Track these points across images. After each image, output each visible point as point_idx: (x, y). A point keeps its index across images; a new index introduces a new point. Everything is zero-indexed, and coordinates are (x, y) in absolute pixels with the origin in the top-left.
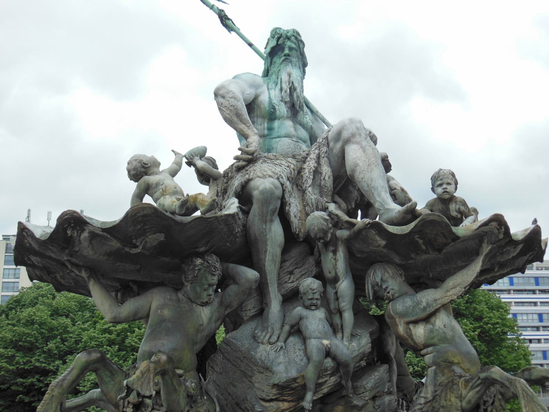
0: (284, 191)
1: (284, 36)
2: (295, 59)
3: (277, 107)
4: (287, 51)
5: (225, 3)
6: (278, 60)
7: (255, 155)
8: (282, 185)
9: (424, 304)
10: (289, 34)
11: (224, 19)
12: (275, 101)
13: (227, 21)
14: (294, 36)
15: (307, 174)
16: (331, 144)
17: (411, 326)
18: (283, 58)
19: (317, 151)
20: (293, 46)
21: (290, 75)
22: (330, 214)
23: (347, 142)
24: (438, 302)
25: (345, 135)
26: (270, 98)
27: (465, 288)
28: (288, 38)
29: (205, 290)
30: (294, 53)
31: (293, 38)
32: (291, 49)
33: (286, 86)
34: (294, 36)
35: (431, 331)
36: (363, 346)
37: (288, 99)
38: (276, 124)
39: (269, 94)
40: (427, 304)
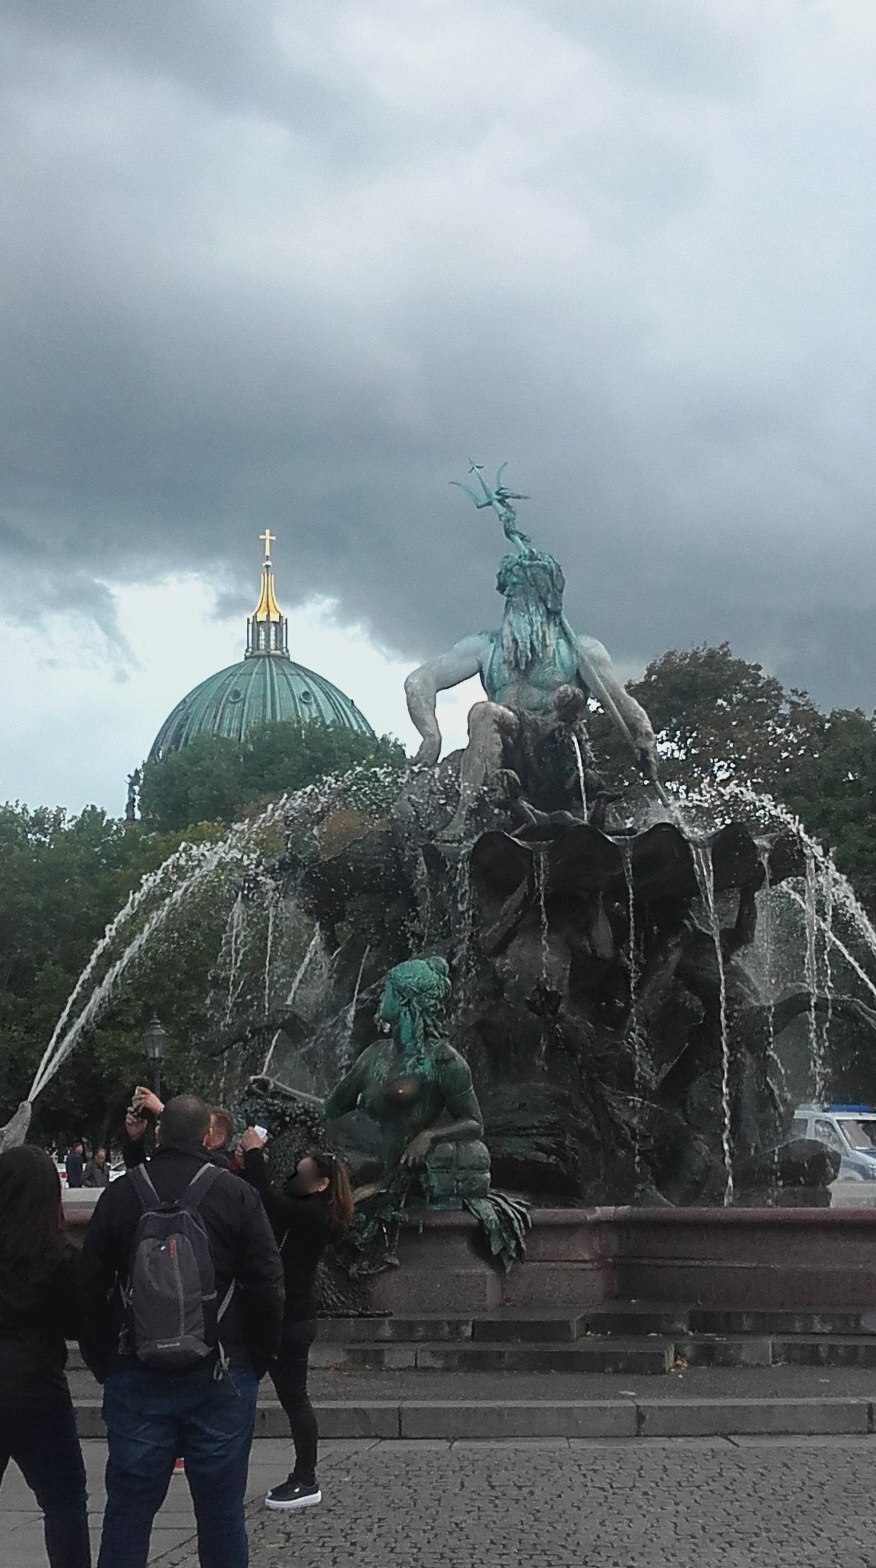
5: (526, 498)
20: (515, 580)
34: (517, 564)
37: (512, 659)
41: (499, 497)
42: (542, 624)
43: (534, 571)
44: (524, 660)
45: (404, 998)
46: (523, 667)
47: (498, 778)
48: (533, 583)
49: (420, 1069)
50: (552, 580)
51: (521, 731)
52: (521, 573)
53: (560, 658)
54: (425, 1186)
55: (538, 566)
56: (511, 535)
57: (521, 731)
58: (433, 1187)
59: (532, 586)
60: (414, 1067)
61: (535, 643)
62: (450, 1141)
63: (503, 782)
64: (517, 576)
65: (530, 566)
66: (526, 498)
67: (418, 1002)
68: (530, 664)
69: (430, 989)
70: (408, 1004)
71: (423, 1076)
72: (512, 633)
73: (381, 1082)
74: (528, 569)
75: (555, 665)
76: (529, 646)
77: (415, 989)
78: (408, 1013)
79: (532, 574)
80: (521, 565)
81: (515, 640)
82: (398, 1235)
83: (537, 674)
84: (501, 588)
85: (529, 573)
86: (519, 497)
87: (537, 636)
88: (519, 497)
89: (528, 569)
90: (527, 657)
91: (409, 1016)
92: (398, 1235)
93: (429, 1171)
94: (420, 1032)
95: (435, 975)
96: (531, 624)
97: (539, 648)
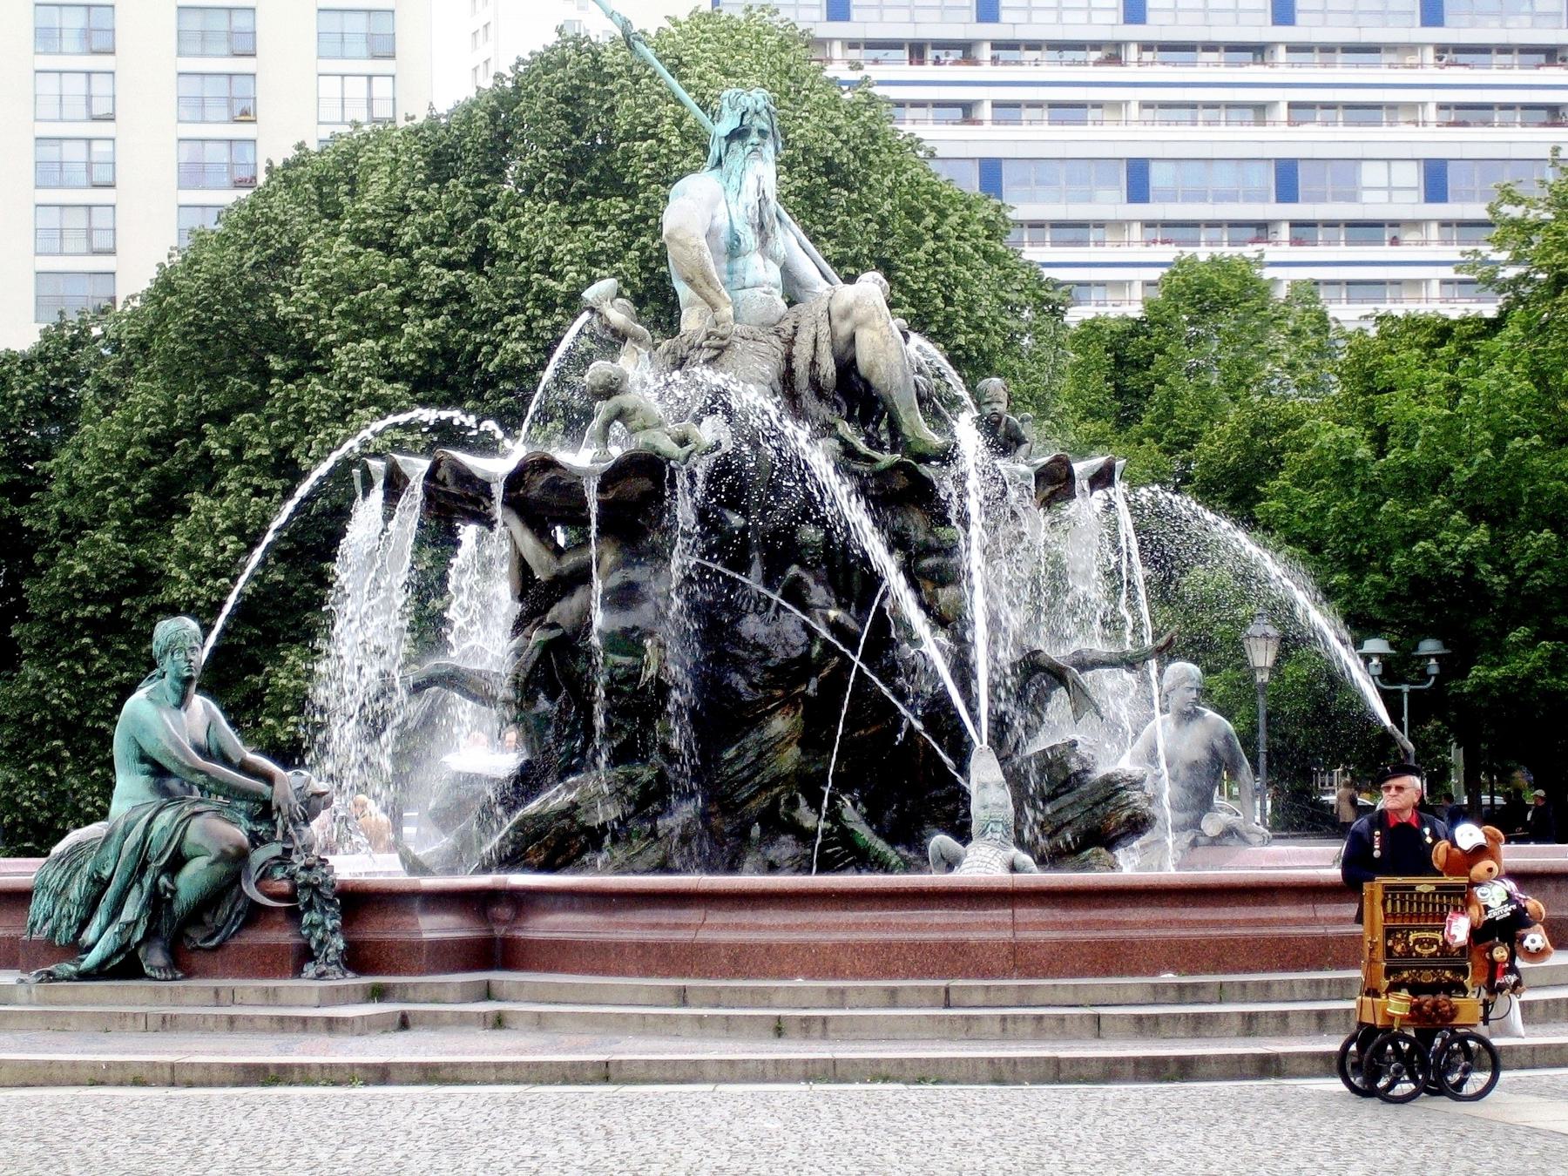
1: (751, 111)
4: (754, 138)
6: (735, 145)
10: (759, 107)
12: (738, 226)
15: (801, 365)
16: (835, 321)
18: (750, 148)
19: (813, 331)
20: (766, 127)
22: (843, 442)
23: (860, 324)
25: (859, 313)
28: (757, 113)
32: (762, 133)
38: (740, 264)
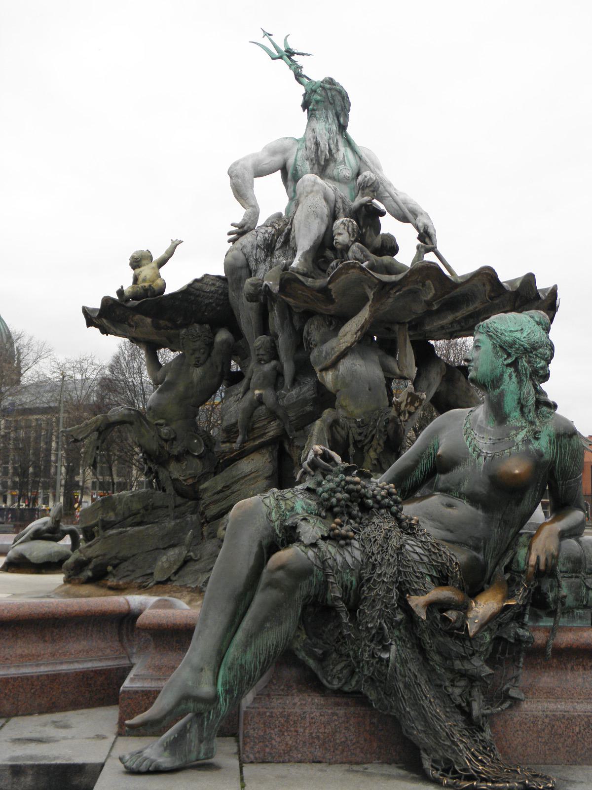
0: (247, 260)
2: (320, 112)
3: (299, 168)
5: (309, 55)
7: (246, 228)
8: (245, 255)
9: (324, 353)
11: (299, 76)
12: (299, 163)
13: (300, 78)
14: (321, 86)
17: (324, 373)
20: (319, 98)
21: (314, 131)
24: (336, 349)
26: (296, 160)
27: (356, 333)
29: (192, 354)
30: (321, 105)
31: (319, 91)
32: (317, 102)
33: (310, 144)
35: (337, 377)
36: (303, 394)
39: (297, 154)
40: (326, 352)
41: (287, 54)
42: (336, 133)
43: (334, 93)
44: (323, 157)
45: (509, 355)
46: (322, 163)
47: (345, 224)
48: (332, 101)
49: (535, 445)
50: (344, 102)
51: (336, 201)
52: (323, 93)
53: (348, 160)
54: (551, 596)
55: (336, 90)
56: (300, 78)
57: (336, 201)
58: (565, 597)
59: (331, 104)
60: (526, 441)
61: (332, 146)
62: (570, 537)
63: (348, 227)
64: (320, 95)
65: (330, 89)
66: (309, 55)
67: (529, 362)
68: (327, 161)
69: (540, 347)
70: (514, 364)
71: (541, 455)
72: (315, 137)
73: (481, 459)
74: (328, 91)
75: (345, 165)
76: (327, 146)
77: (527, 346)
78: (514, 375)
79: (332, 95)
80: (323, 88)
81: (317, 144)
82: (522, 659)
83: (332, 170)
84: (305, 106)
85: (329, 94)
86: (303, 54)
87: (333, 141)
88: (303, 54)
89: (328, 91)
90: (326, 156)
91: (514, 379)
92: (522, 659)
93: (560, 575)
94: (532, 401)
95: (542, 331)
96: (329, 131)
97: (334, 151)
